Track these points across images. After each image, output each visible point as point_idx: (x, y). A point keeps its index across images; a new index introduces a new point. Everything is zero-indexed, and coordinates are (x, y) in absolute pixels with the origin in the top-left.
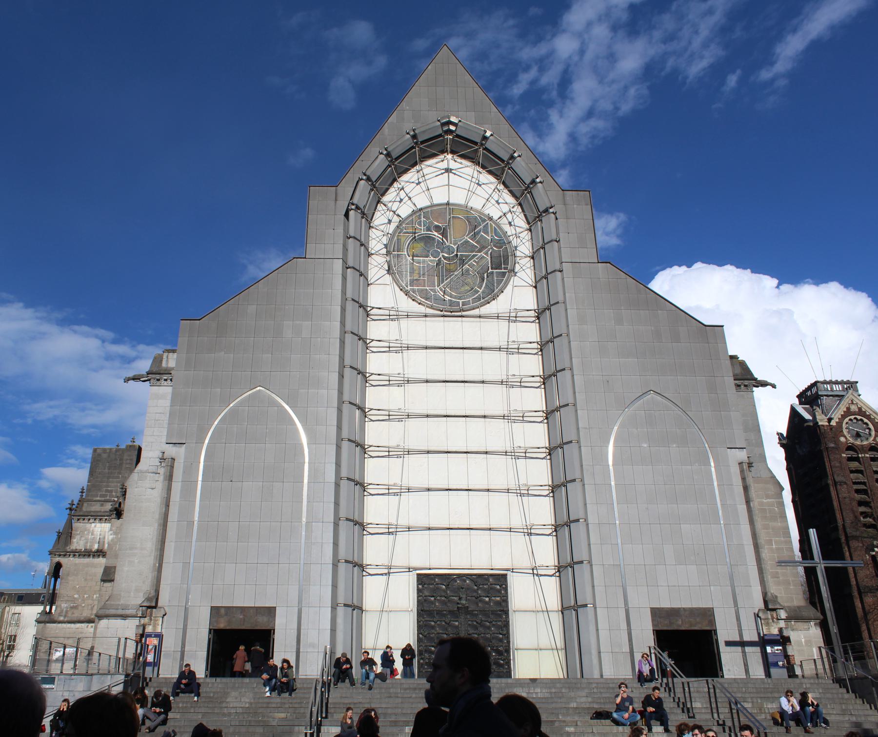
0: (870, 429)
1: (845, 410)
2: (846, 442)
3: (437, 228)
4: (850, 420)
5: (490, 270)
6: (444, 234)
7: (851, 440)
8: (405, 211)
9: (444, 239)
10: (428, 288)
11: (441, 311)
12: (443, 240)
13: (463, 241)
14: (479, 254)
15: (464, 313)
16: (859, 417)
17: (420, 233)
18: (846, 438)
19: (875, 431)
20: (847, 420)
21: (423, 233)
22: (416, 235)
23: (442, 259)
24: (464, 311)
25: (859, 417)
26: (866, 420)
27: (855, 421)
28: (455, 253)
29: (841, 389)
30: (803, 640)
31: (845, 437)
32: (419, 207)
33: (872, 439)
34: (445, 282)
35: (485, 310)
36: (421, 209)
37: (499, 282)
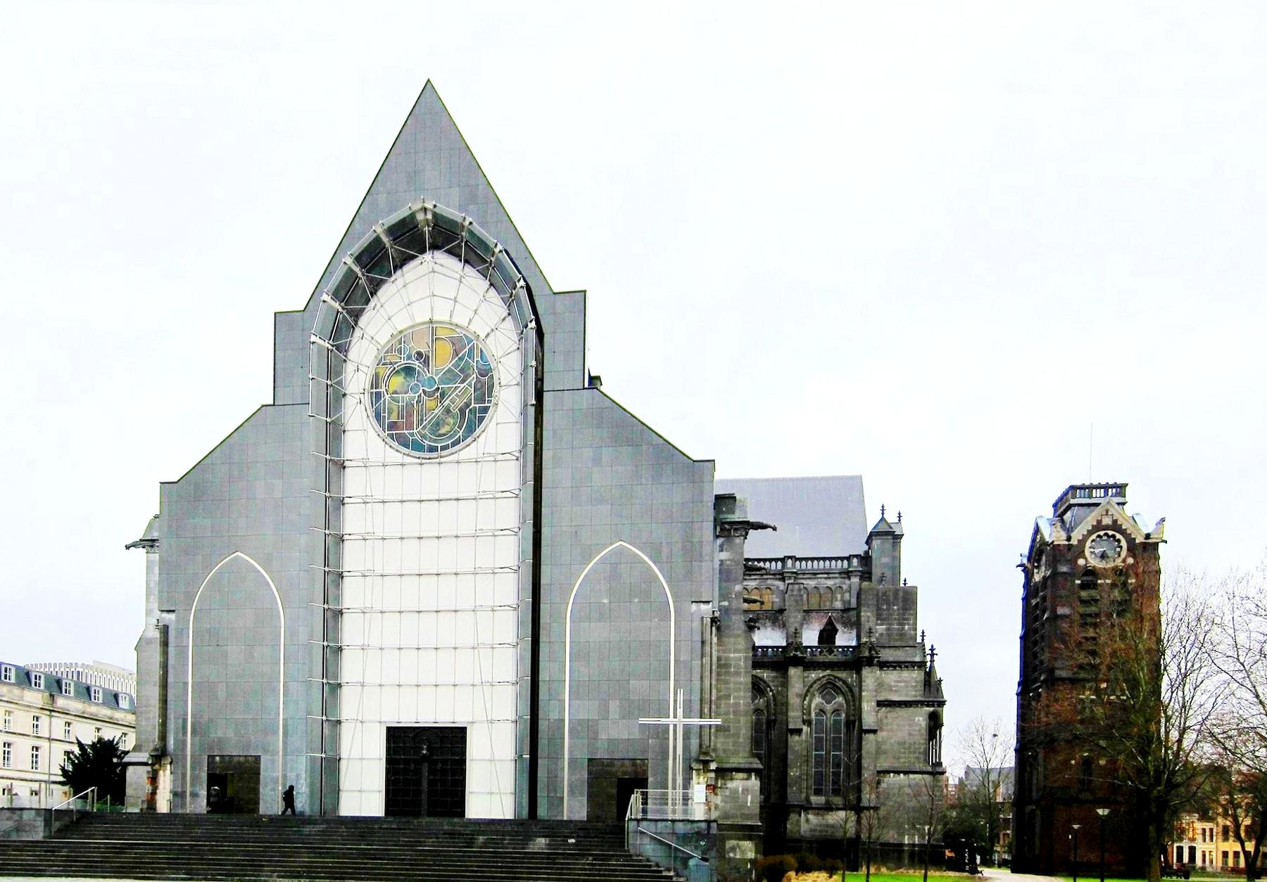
0: (1121, 547)
1: (1095, 523)
2: (1086, 565)
3: (419, 354)
4: (1099, 536)
5: (473, 405)
6: (426, 363)
7: (1092, 562)
8: (383, 338)
9: (425, 369)
10: (406, 432)
11: (419, 458)
12: (424, 371)
13: (445, 370)
14: (462, 386)
15: (442, 460)
16: (1110, 533)
17: (400, 363)
18: (1091, 559)
19: (1128, 550)
20: (1094, 537)
21: (403, 362)
22: (396, 366)
23: (423, 395)
24: (441, 457)
25: (1110, 533)
26: (1118, 536)
27: (1105, 538)
28: (436, 386)
29: (1094, 490)
30: (740, 789)
31: (1086, 559)
32: (399, 330)
33: (1120, 560)
34: (425, 423)
35: (464, 455)
36: (401, 332)
37: (481, 420)
